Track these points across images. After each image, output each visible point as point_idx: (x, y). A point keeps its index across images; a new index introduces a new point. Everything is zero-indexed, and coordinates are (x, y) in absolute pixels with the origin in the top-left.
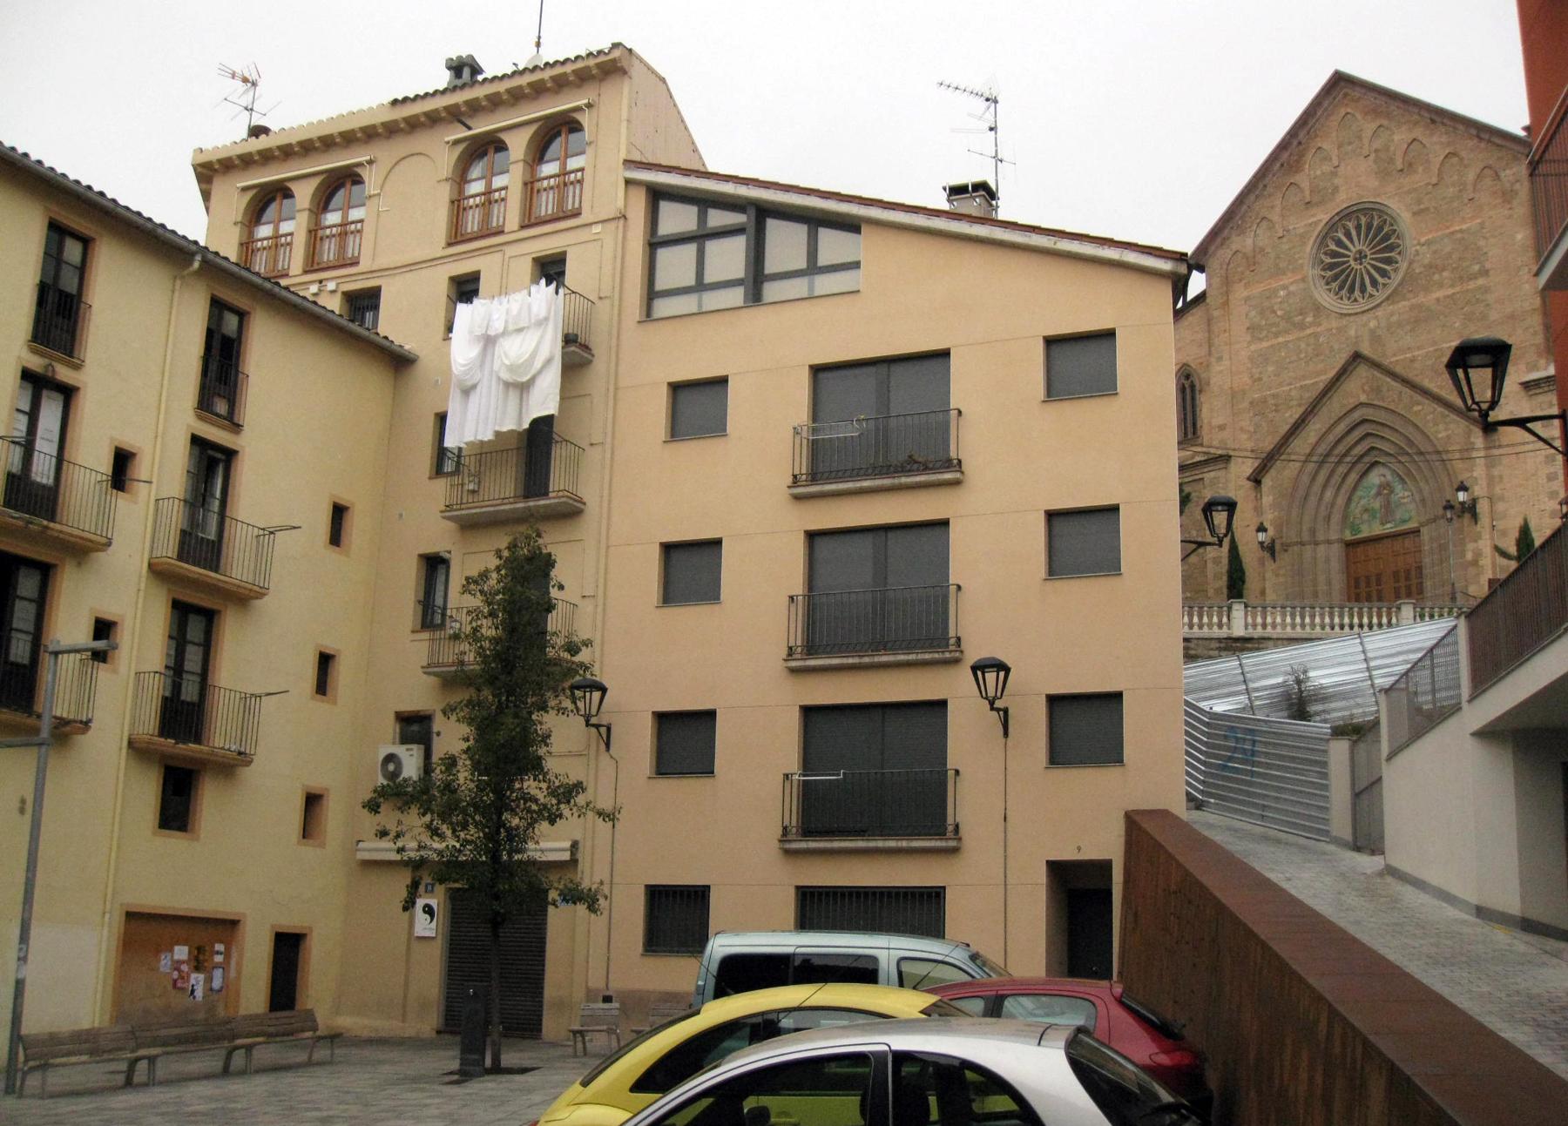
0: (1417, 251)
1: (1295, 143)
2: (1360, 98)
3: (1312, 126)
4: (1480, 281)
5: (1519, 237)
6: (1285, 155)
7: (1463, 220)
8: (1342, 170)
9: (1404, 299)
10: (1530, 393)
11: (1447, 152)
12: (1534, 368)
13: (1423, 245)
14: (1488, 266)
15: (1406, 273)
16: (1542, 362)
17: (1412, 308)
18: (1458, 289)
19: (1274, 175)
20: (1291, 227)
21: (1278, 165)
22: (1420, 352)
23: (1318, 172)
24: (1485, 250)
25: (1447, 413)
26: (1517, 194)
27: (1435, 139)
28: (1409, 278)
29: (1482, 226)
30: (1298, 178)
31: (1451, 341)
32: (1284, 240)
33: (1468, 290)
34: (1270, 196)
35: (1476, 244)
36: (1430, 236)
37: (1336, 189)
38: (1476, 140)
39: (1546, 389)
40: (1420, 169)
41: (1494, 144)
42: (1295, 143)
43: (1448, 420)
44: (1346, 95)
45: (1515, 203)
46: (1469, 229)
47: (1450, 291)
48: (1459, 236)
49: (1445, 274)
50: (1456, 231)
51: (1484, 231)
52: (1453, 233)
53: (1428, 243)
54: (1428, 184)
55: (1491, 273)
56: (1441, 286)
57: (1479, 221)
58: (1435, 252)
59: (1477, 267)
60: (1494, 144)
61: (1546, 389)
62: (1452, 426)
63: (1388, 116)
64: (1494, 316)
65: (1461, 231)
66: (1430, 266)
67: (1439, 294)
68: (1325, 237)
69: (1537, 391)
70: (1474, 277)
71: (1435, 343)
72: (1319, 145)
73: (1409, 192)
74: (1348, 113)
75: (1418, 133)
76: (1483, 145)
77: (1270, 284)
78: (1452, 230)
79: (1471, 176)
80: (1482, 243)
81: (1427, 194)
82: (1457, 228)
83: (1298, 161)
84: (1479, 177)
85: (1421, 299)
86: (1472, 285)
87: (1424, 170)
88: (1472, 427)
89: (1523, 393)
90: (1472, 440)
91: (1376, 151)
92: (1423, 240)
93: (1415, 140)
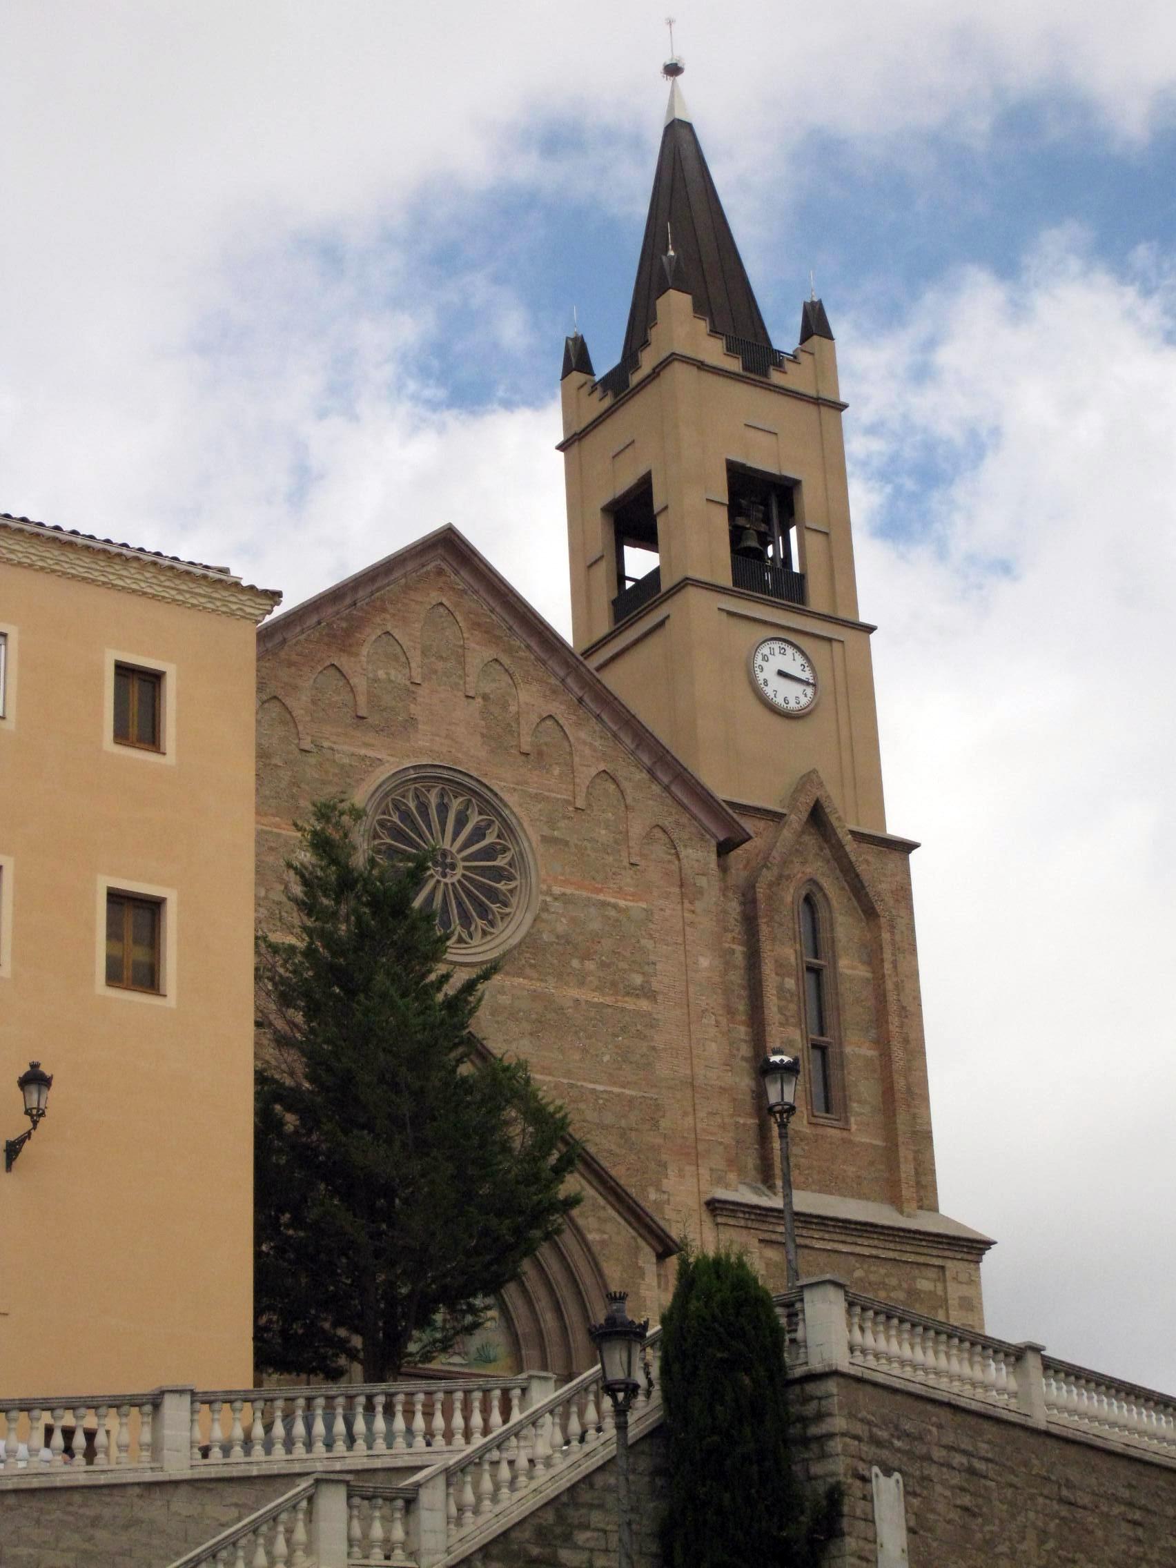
0: (545, 902)
1: (348, 601)
2: (464, 591)
3: (378, 590)
4: (644, 1005)
5: (704, 962)
6: (330, 610)
7: (620, 892)
8: (422, 692)
9: (520, 973)
10: (719, 1220)
11: (602, 767)
12: (720, 1181)
13: (556, 899)
14: (655, 986)
15: (529, 934)
16: (732, 1177)
17: (535, 996)
18: (608, 1000)
19: (302, 632)
20: (326, 744)
21: (314, 619)
22: (548, 1078)
23: (381, 674)
24: (652, 958)
25: (601, 1201)
26: (701, 893)
27: (583, 735)
28: (530, 943)
29: (649, 913)
30: (343, 661)
31: (600, 1083)
32: (312, 760)
33: (623, 1010)
34: (291, 664)
35: (638, 942)
36: (568, 891)
37: (412, 721)
38: (645, 775)
39: (742, 1223)
40: (556, 771)
41: (674, 798)
42: (348, 601)
43: (602, 1214)
44: (440, 572)
45: (699, 906)
46: (627, 909)
47: (597, 998)
48: (613, 913)
49: (590, 965)
50: (609, 904)
51: (651, 926)
52: (604, 904)
53: (564, 899)
54: (568, 802)
55: (660, 998)
56: (582, 984)
57: (644, 906)
58: (573, 920)
59: (638, 980)
60: (674, 798)
61: (742, 1223)
62: (609, 1227)
63: (510, 651)
64: (663, 1070)
65: (615, 906)
66: (565, 939)
67: (574, 993)
68: (387, 795)
69: (731, 1221)
70: (631, 992)
71: (568, 1073)
72: (389, 628)
73: (537, 798)
74: (441, 604)
75: (557, 708)
76: (656, 788)
77: (278, 826)
78: (601, 897)
79: (637, 829)
80: (647, 943)
81: (565, 817)
82: (613, 900)
83: (348, 633)
84: (648, 837)
85: (550, 987)
86: (630, 1004)
87: (560, 775)
88: (639, 1240)
89: (706, 1217)
90: (641, 1263)
91: (485, 697)
92: (557, 890)
93: (550, 716)
